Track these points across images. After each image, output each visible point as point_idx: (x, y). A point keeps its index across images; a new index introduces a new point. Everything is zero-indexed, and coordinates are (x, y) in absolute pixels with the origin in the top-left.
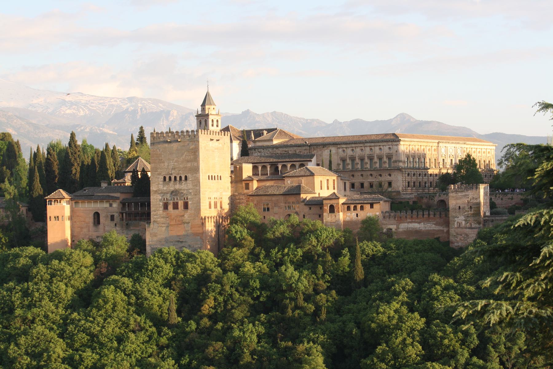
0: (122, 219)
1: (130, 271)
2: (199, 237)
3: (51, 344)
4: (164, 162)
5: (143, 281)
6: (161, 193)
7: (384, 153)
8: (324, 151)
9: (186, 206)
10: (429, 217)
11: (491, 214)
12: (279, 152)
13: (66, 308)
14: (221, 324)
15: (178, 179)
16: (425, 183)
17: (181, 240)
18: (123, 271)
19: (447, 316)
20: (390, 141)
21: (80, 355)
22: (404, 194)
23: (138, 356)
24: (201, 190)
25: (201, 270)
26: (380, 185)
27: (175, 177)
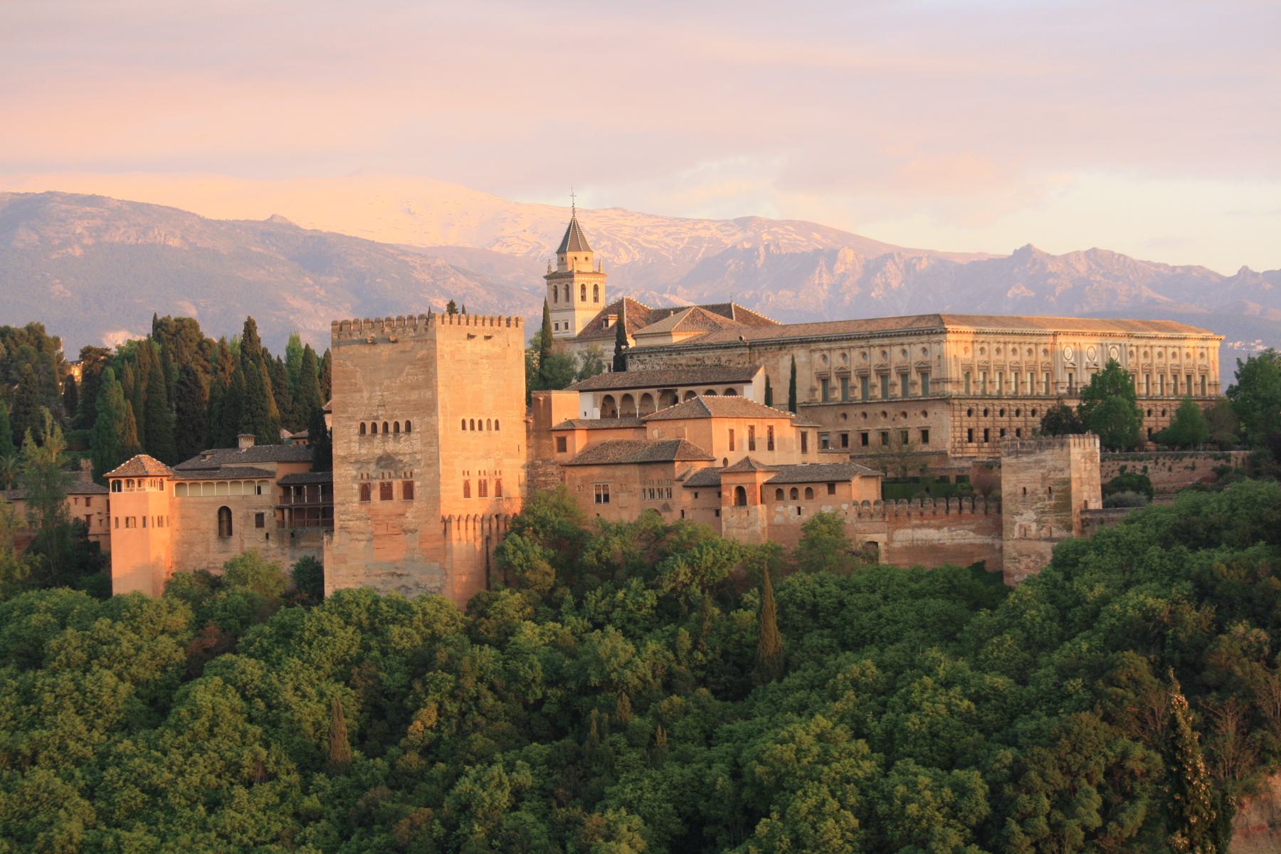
0: (281, 524)
1: (265, 644)
2: (437, 565)
3: (62, 812)
4: (360, 391)
5: (286, 668)
6: (357, 462)
7: (913, 362)
8: (782, 357)
9: (409, 492)
10: (960, 513)
11: (1106, 505)
12: (683, 362)
13: (110, 731)
14: (441, 766)
15: (391, 428)
16: (1003, 432)
17: (399, 572)
18: (250, 643)
19: (934, 748)
20: (923, 334)
21: (117, 838)
22: (955, 458)
23: (245, 840)
24: (443, 454)
25: (425, 640)
26: (905, 435)
27: (386, 425)
